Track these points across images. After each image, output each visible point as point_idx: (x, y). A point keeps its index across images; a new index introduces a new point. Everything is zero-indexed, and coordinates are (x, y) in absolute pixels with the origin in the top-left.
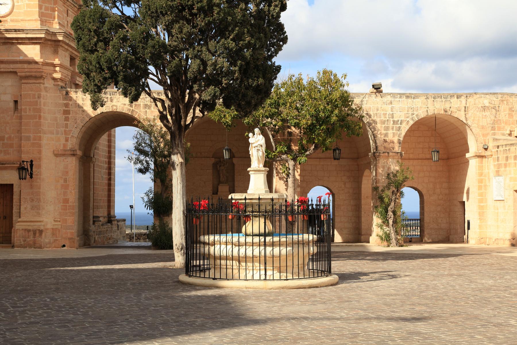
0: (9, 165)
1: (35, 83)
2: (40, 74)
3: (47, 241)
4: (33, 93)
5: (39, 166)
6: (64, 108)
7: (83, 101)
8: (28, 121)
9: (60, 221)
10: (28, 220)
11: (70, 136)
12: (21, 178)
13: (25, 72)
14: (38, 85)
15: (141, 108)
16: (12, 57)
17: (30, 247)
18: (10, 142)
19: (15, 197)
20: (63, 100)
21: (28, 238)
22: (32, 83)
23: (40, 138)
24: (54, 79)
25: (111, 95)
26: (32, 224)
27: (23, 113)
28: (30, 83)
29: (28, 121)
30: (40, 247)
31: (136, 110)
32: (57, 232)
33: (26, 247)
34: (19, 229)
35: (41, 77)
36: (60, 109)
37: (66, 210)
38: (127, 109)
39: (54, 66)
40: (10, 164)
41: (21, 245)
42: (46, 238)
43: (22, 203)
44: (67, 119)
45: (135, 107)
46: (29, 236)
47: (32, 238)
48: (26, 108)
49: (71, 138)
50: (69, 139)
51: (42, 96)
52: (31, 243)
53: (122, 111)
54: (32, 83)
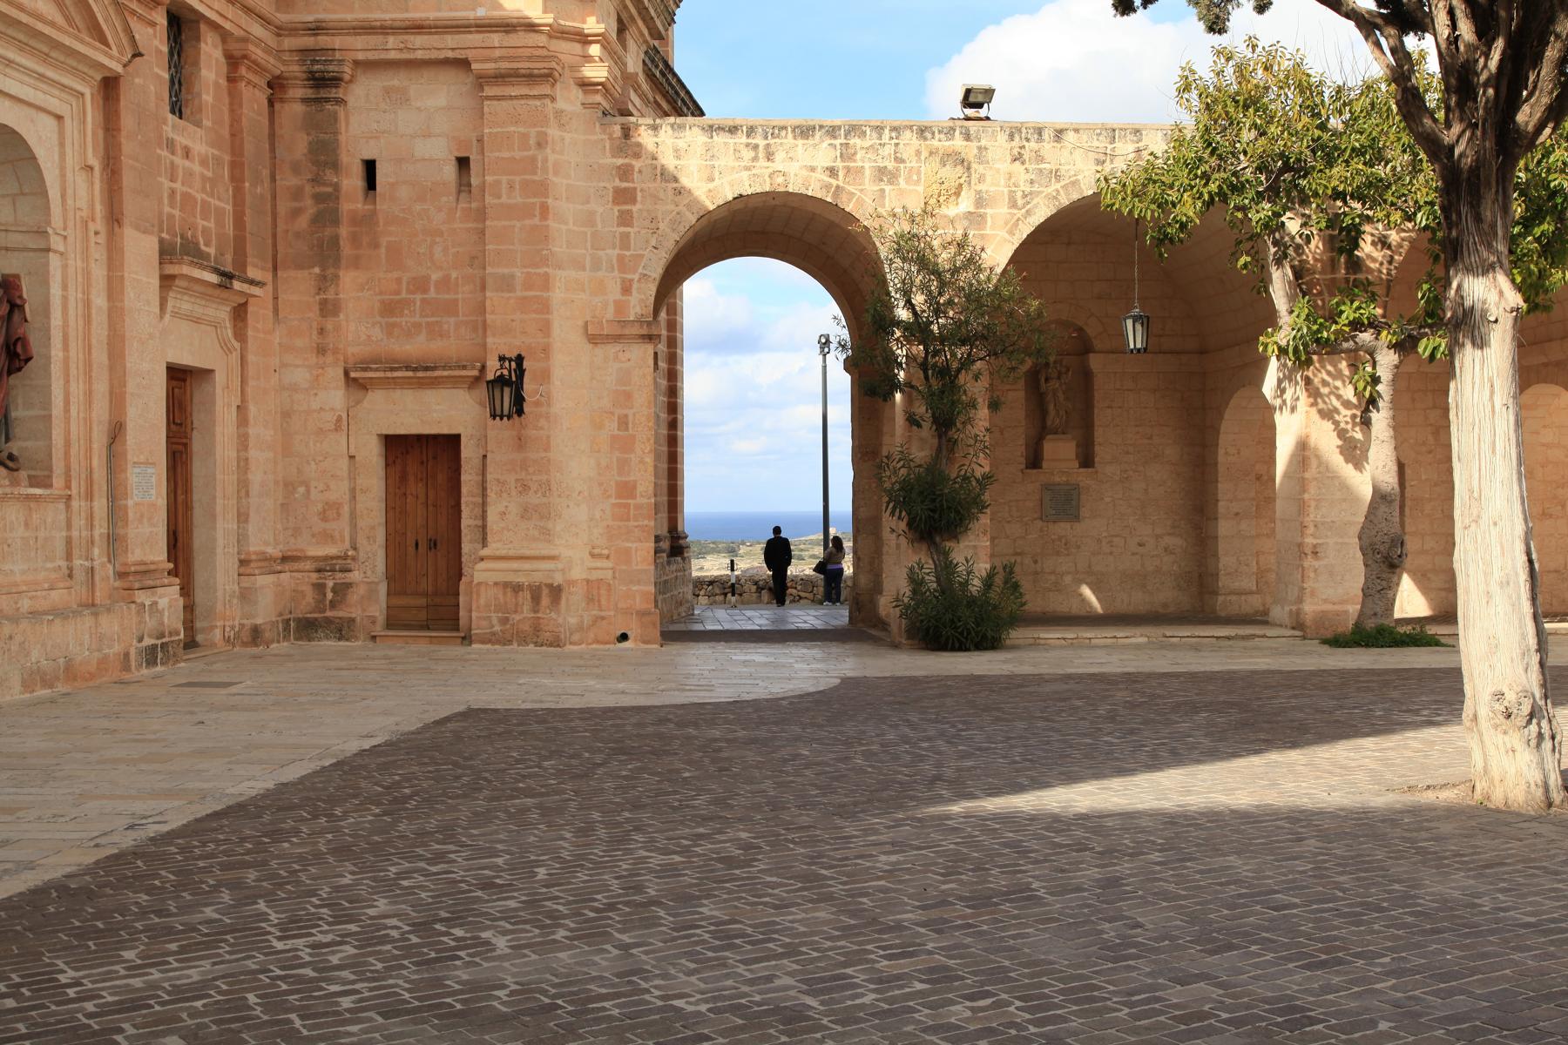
0: (446, 373)
1: (527, 97)
2: (546, 65)
3: (573, 621)
4: (521, 130)
5: (545, 376)
6: (617, 183)
7: (678, 158)
8: (506, 223)
9: (608, 557)
10: (512, 553)
11: (636, 277)
12: (498, 412)
13: (495, 60)
14: (538, 103)
15: (867, 180)
16: (451, 10)
17: (524, 641)
18: (446, 296)
19: (468, 478)
20: (613, 156)
21: (516, 612)
22: (516, 97)
23: (546, 284)
24: (585, 85)
25: (766, 138)
26: (527, 565)
27: (489, 199)
28: (511, 98)
29: (506, 223)
30: (556, 643)
31: (851, 188)
32: (603, 592)
33: (510, 642)
34: (487, 584)
35: (548, 77)
36: (602, 184)
37: (628, 520)
38: (818, 185)
39: (584, 39)
40: (450, 368)
41: (494, 634)
42: (571, 614)
43: (491, 495)
44: (625, 219)
45: (845, 176)
46: (517, 604)
47: (526, 612)
48: (498, 182)
49: (639, 280)
50: (635, 285)
51: (550, 139)
52: (526, 627)
53: (803, 191)
54: (516, 97)
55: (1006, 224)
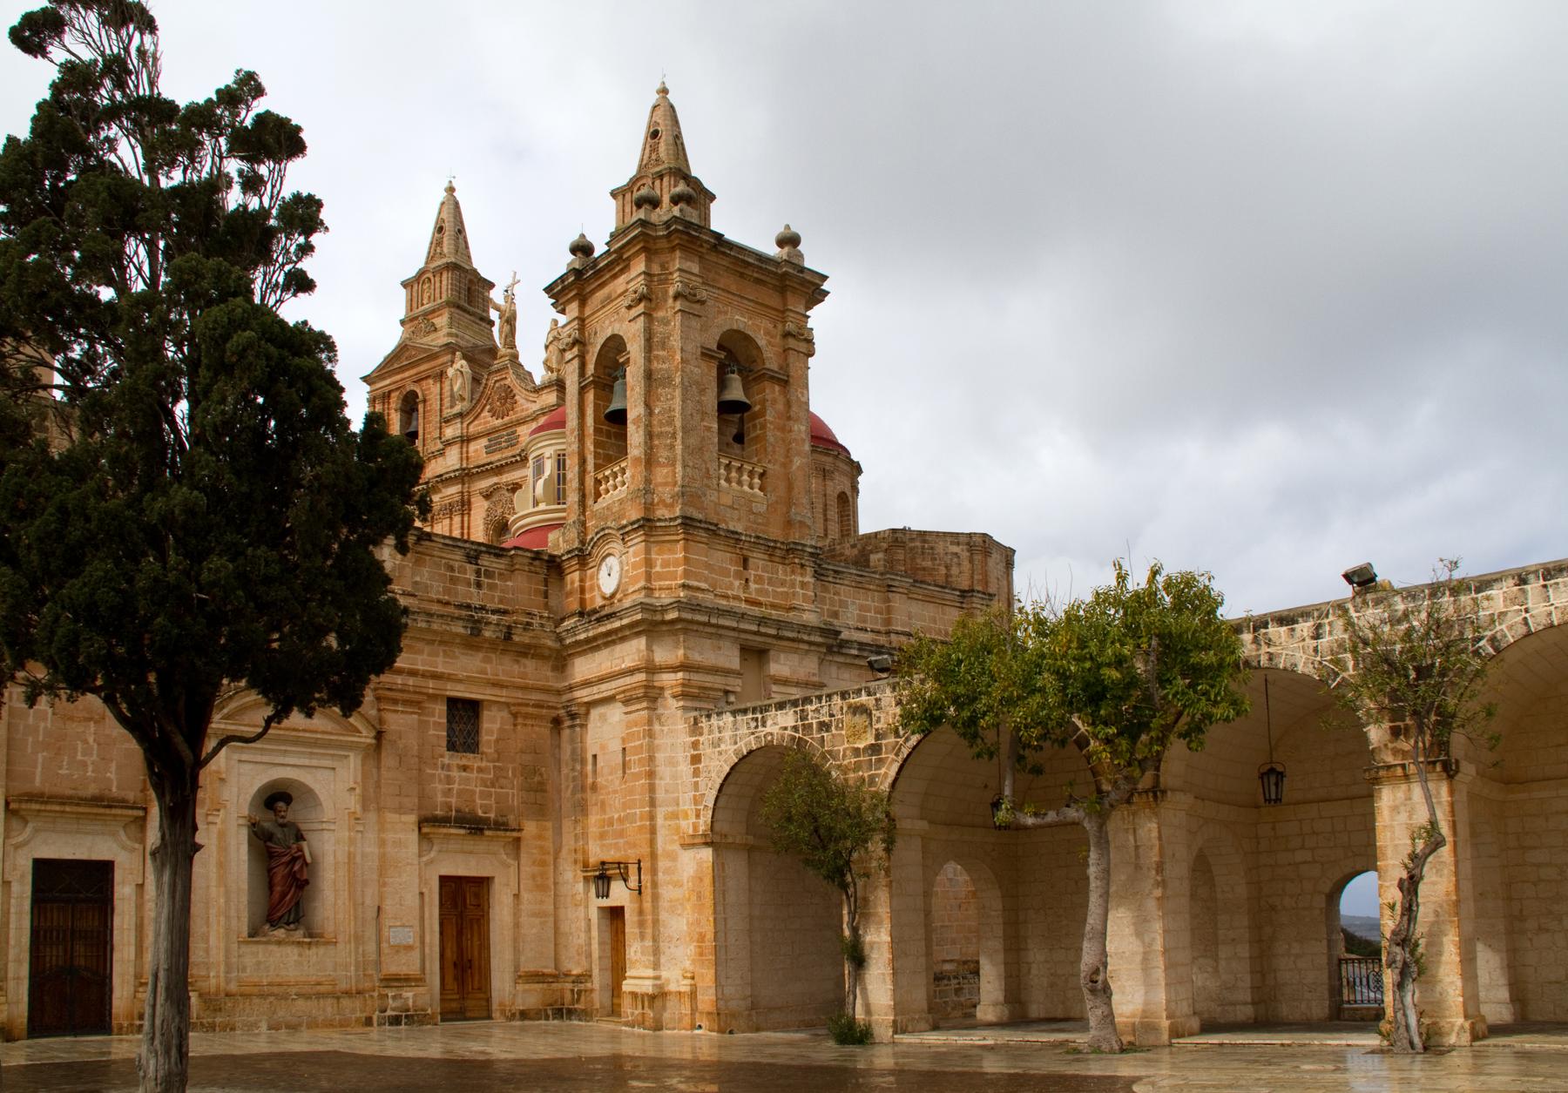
44: (696, 773)
55: (894, 749)
